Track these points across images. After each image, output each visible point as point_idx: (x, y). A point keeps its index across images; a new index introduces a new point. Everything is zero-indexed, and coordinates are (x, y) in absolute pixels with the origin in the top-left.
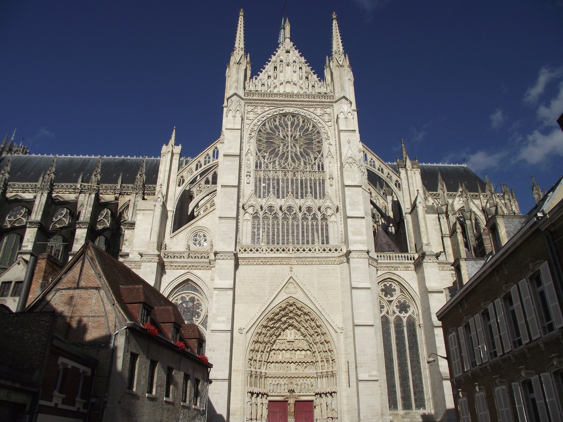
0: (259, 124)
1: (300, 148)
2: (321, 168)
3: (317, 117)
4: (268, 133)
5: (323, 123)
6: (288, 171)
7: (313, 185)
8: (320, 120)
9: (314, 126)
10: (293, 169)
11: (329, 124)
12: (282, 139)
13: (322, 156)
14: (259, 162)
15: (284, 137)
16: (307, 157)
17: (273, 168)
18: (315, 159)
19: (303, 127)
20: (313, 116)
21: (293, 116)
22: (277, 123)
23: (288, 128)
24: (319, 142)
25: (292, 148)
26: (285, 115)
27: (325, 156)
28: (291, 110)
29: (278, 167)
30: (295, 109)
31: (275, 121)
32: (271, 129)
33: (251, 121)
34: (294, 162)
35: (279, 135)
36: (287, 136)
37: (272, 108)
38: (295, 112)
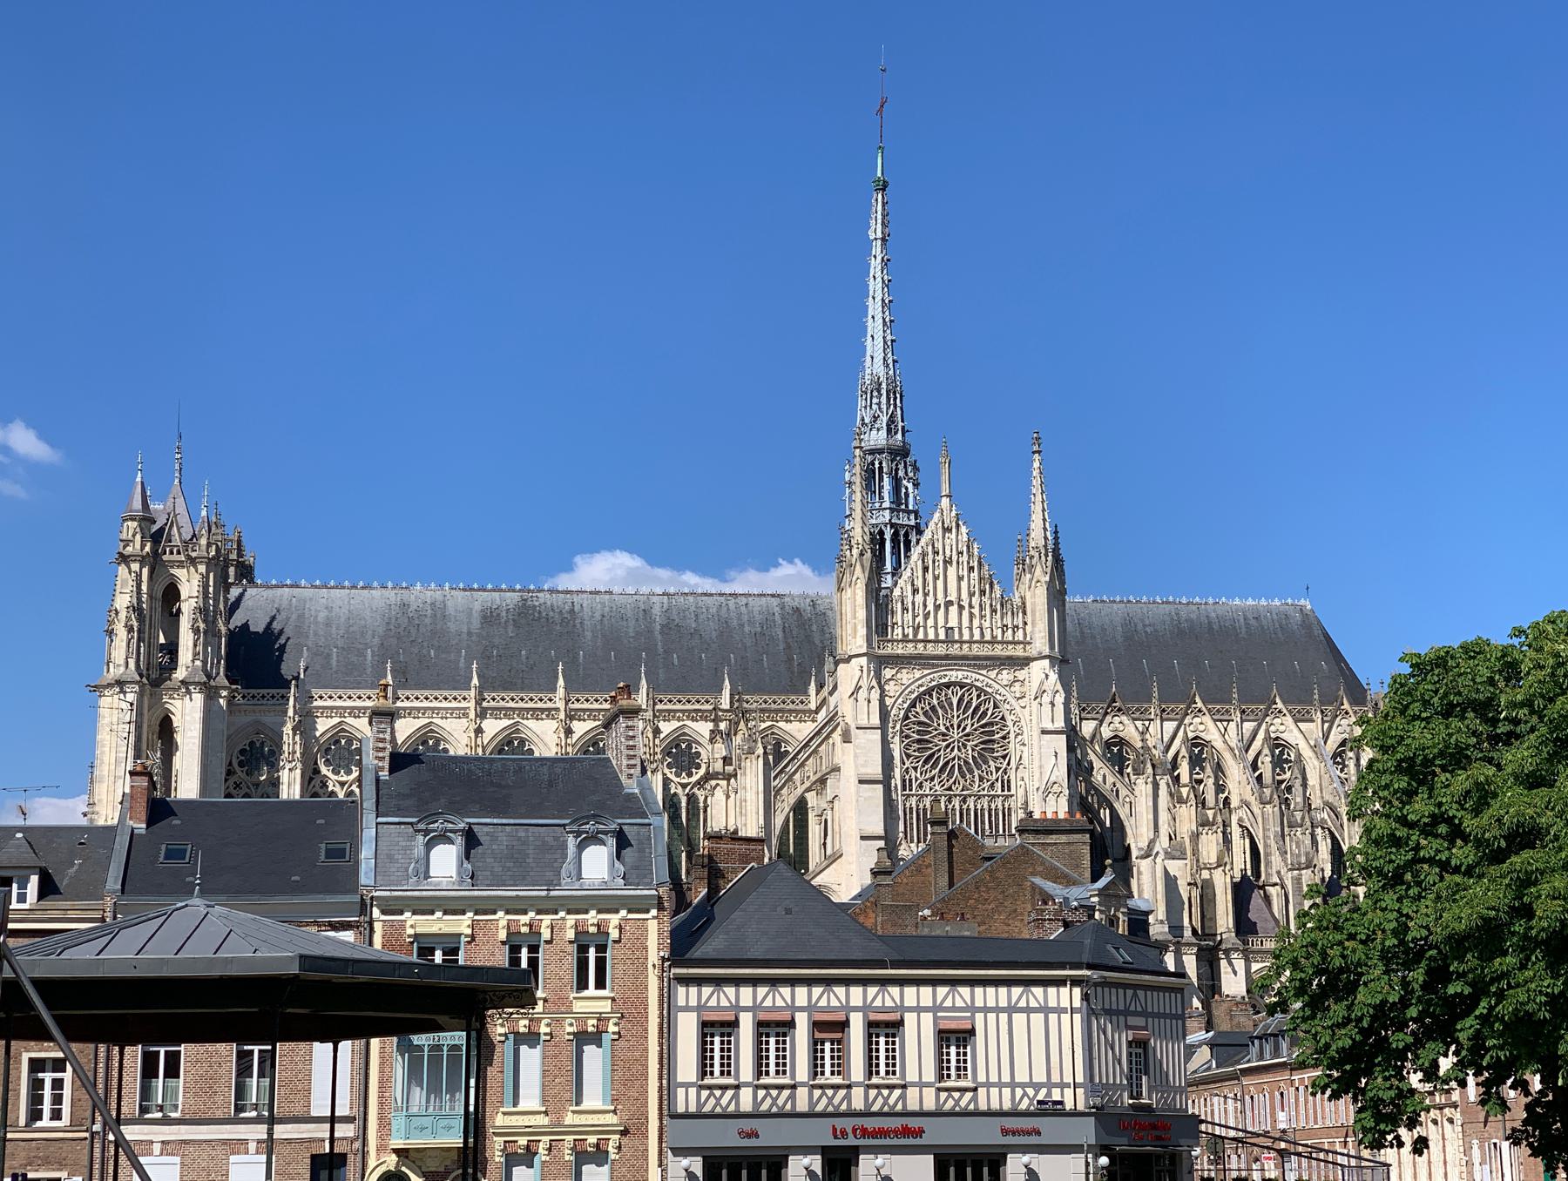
0: (906, 706)
1: (973, 750)
2: (1007, 785)
3: (1002, 690)
4: (920, 723)
5: (1013, 701)
6: (955, 796)
7: (993, 819)
8: (1008, 695)
9: (996, 706)
10: (962, 790)
11: (1022, 702)
12: (944, 735)
13: (1008, 764)
14: (907, 777)
15: (947, 728)
16: (984, 767)
17: (931, 789)
18: (998, 769)
19: (977, 708)
20: (997, 687)
21: (962, 688)
22: (935, 702)
23: (952, 710)
24: (1004, 738)
25: (959, 750)
26: (948, 686)
27: (1013, 764)
28: (955, 675)
29: (937, 787)
30: (966, 673)
31: (931, 696)
32: (925, 713)
33: (894, 699)
34: (963, 777)
35: (939, 725)
36: (952, 725)
37: (926, 672)
38: (965, 681)
